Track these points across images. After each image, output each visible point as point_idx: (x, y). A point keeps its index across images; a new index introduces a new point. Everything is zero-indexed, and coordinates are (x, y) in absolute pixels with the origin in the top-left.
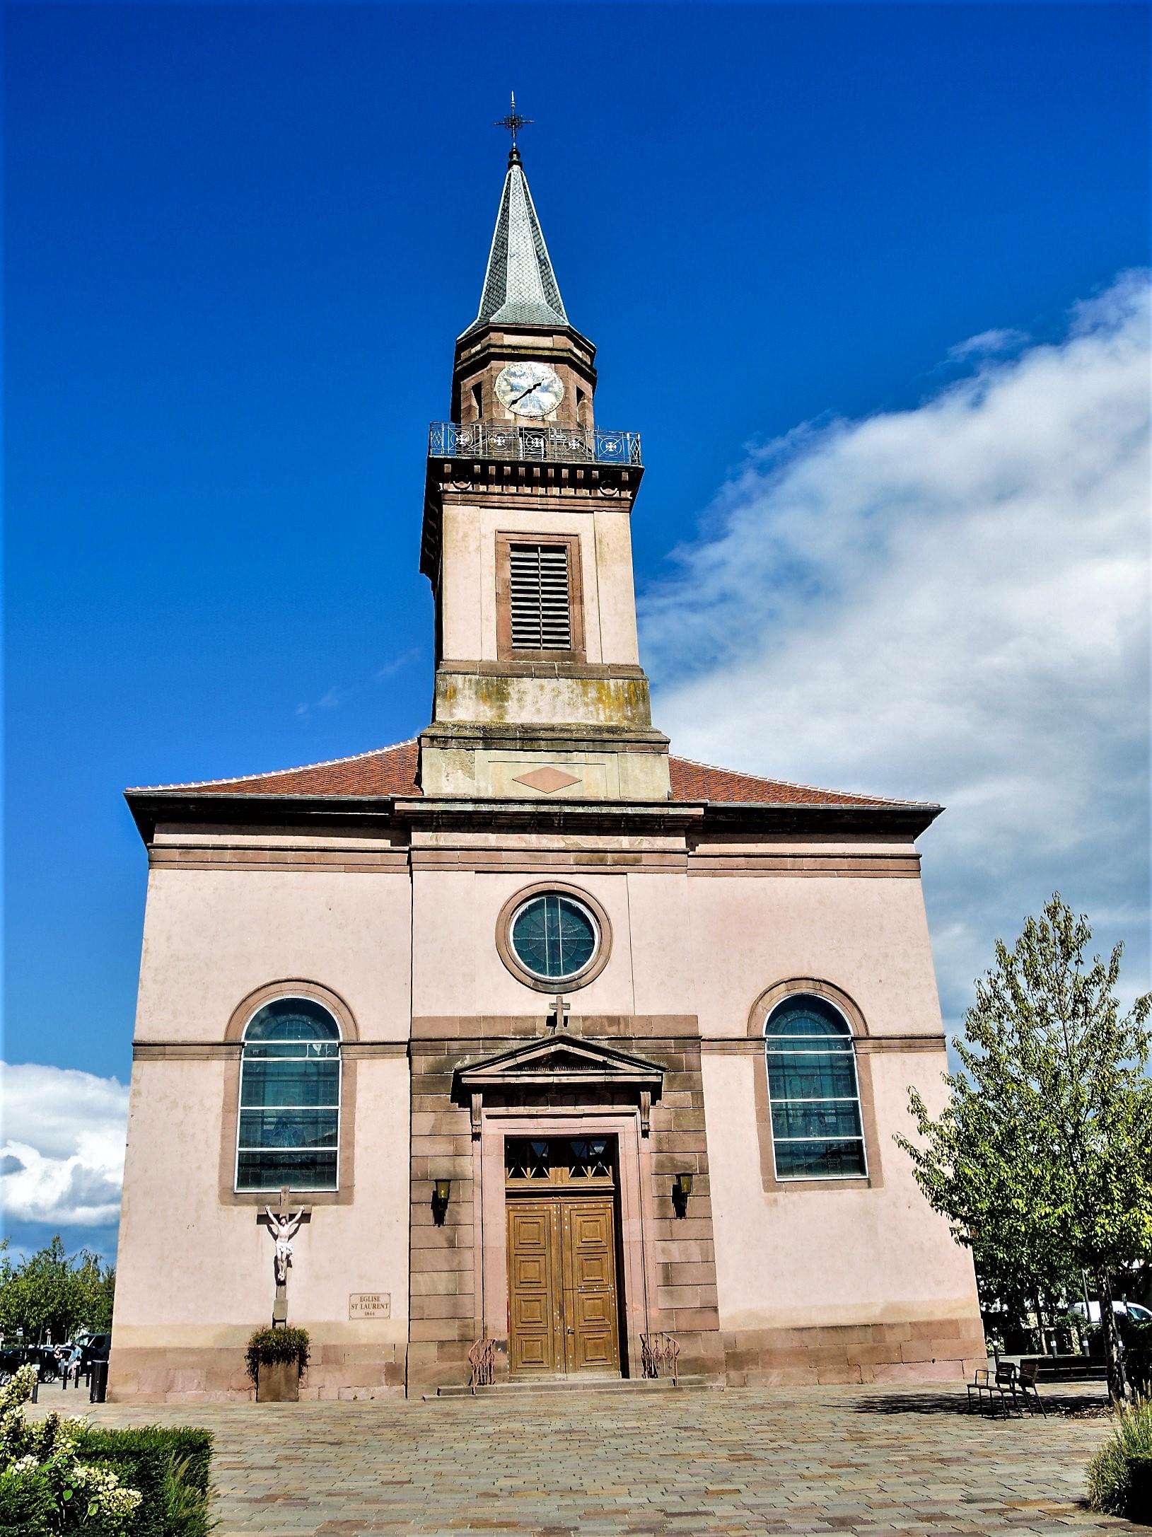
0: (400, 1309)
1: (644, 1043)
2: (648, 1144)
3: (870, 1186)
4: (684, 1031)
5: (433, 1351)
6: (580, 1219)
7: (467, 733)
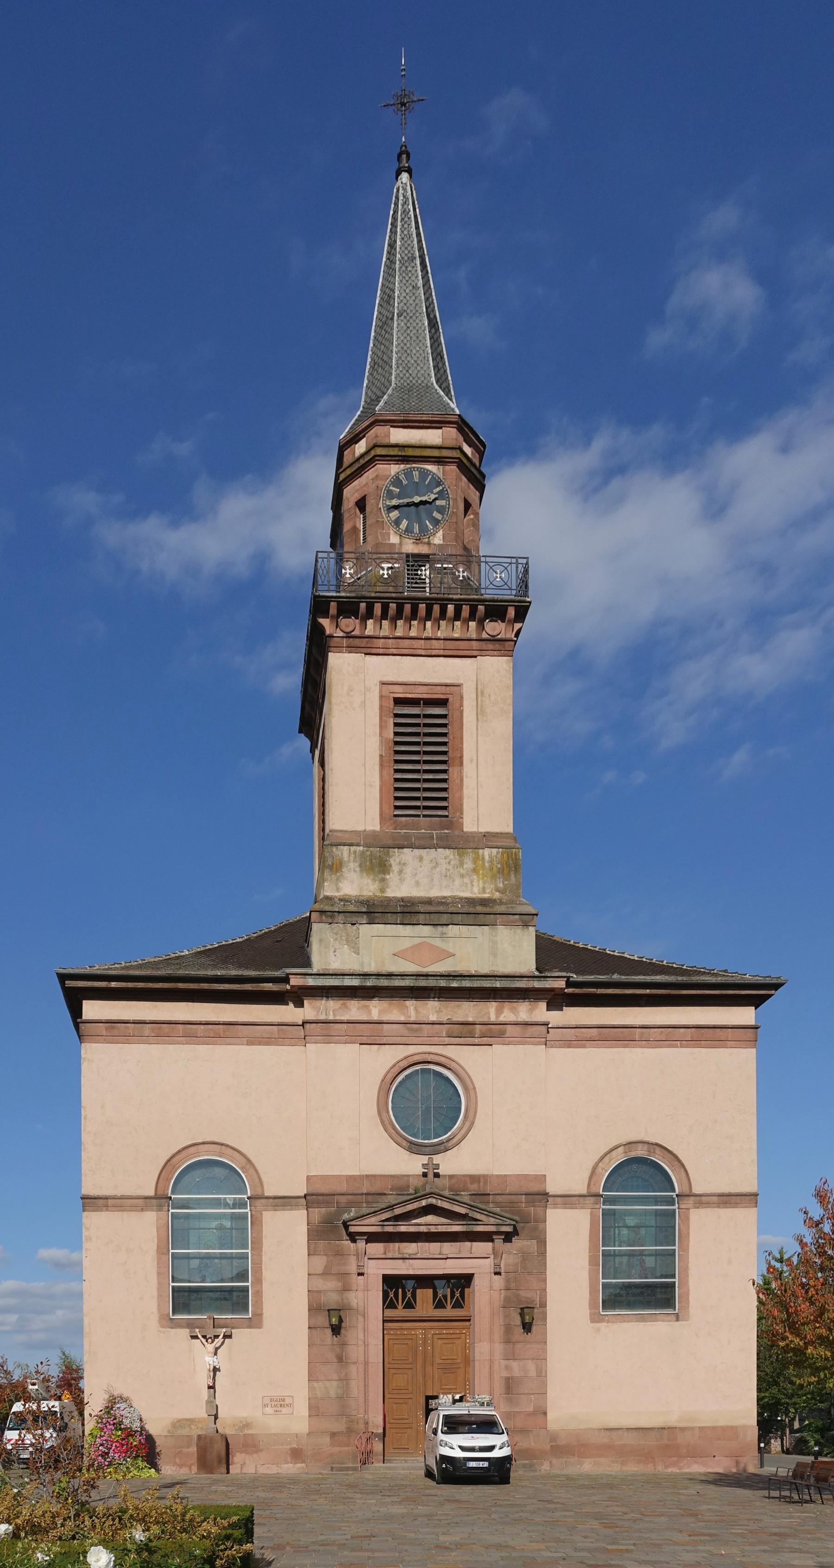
0: (302, 1409)
1: (499, 1199)
2: (499, 1281)
3: (677, 1320)
4: (534, 1188)
5: (327, 1439)
6: (440, 1342)
7: (352, 908)
